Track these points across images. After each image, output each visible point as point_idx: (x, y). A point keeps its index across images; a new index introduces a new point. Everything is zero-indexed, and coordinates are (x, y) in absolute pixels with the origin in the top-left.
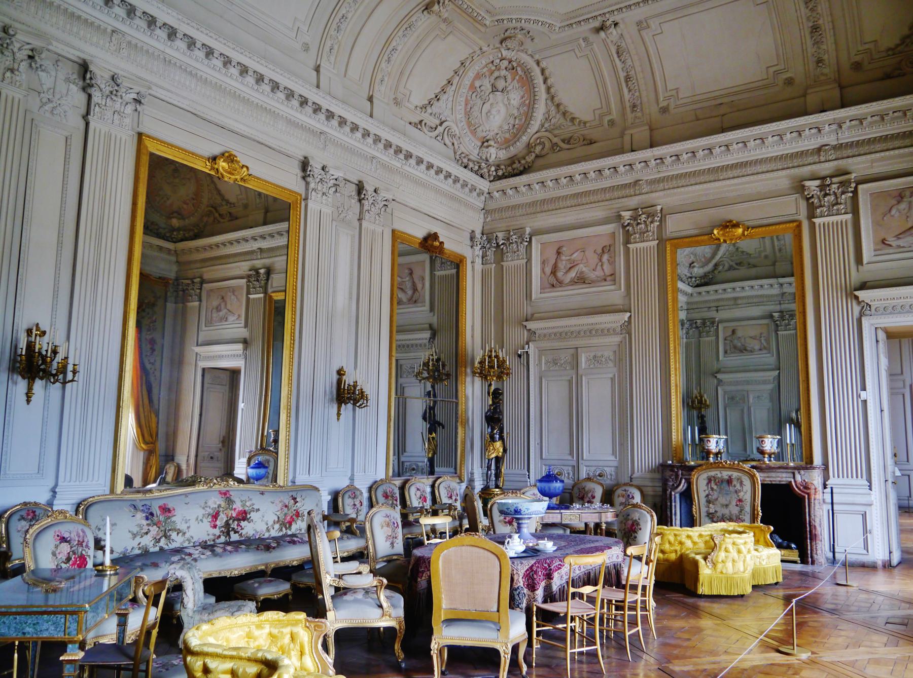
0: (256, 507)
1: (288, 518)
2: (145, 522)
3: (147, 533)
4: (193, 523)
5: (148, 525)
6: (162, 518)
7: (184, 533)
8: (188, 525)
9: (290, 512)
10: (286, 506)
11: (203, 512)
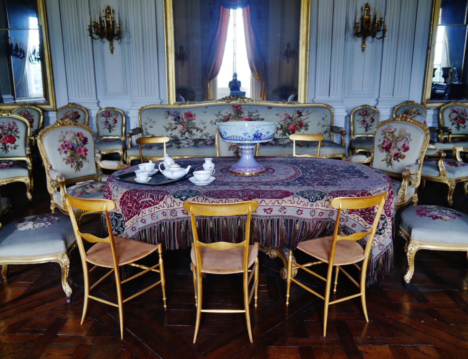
0: (260, 117)
1: (291, 127)
2: (173, 122)
3: (175, 129)
4: (208, 125)
5: (176, 124)
6: (185, 120)
7: (202, 131)
8: (204, 125)
9: (292, 123)
10: (290, 118)
11: (217, 118)
